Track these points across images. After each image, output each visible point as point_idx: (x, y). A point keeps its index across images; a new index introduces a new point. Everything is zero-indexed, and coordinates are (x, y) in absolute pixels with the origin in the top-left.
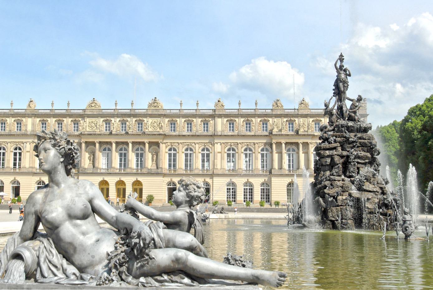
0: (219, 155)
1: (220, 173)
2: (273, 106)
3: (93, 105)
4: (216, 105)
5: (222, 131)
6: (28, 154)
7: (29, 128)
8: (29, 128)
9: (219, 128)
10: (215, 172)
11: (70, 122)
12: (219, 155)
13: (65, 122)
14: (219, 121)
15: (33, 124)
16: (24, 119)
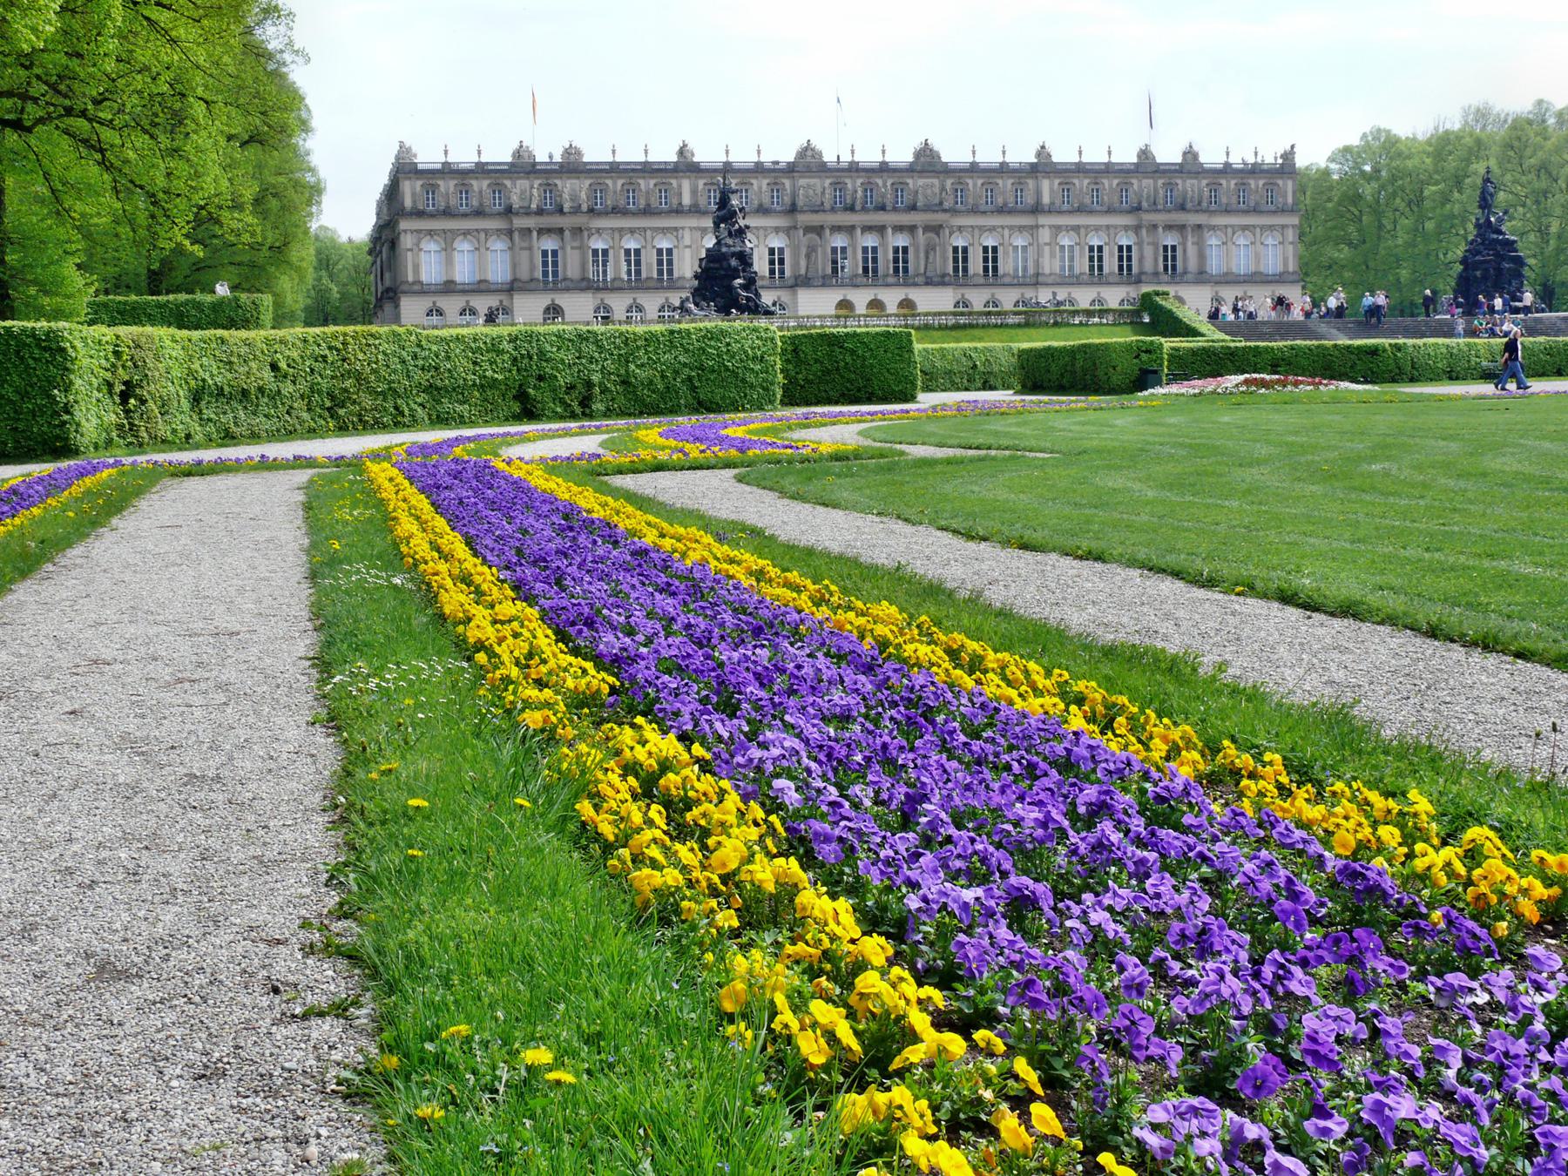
0: (1047, 249)
1: (1050, 280)
2: (1139, 156)
3: (809, 153)
4: (1039, 155)
5: (1052, 203)
6: (688, 251)
7: (687, 200)
8: (687, 200)
9: (1046, 200)
10: (1041, 279)
11: (764, 187)
12: (1047, 249)
13: (755, 187)
14: (1046, 185)
15: (694, 192)
16: (674, 182)
